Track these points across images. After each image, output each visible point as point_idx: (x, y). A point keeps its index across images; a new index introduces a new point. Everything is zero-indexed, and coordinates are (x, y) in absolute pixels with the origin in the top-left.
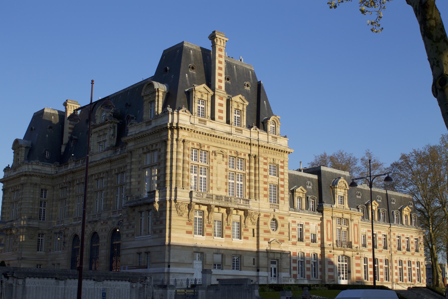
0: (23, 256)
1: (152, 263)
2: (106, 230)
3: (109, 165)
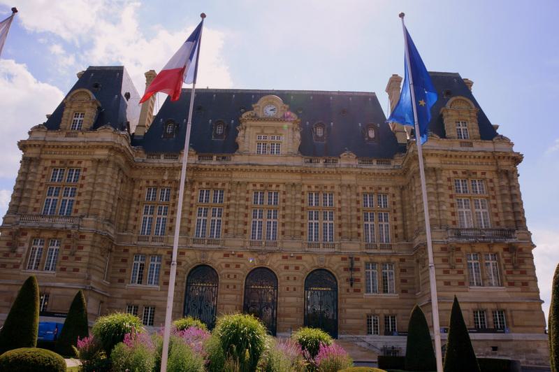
0: (92, 285)
1: (514, 326)
2: (297, 268)
3: (299, 177)
